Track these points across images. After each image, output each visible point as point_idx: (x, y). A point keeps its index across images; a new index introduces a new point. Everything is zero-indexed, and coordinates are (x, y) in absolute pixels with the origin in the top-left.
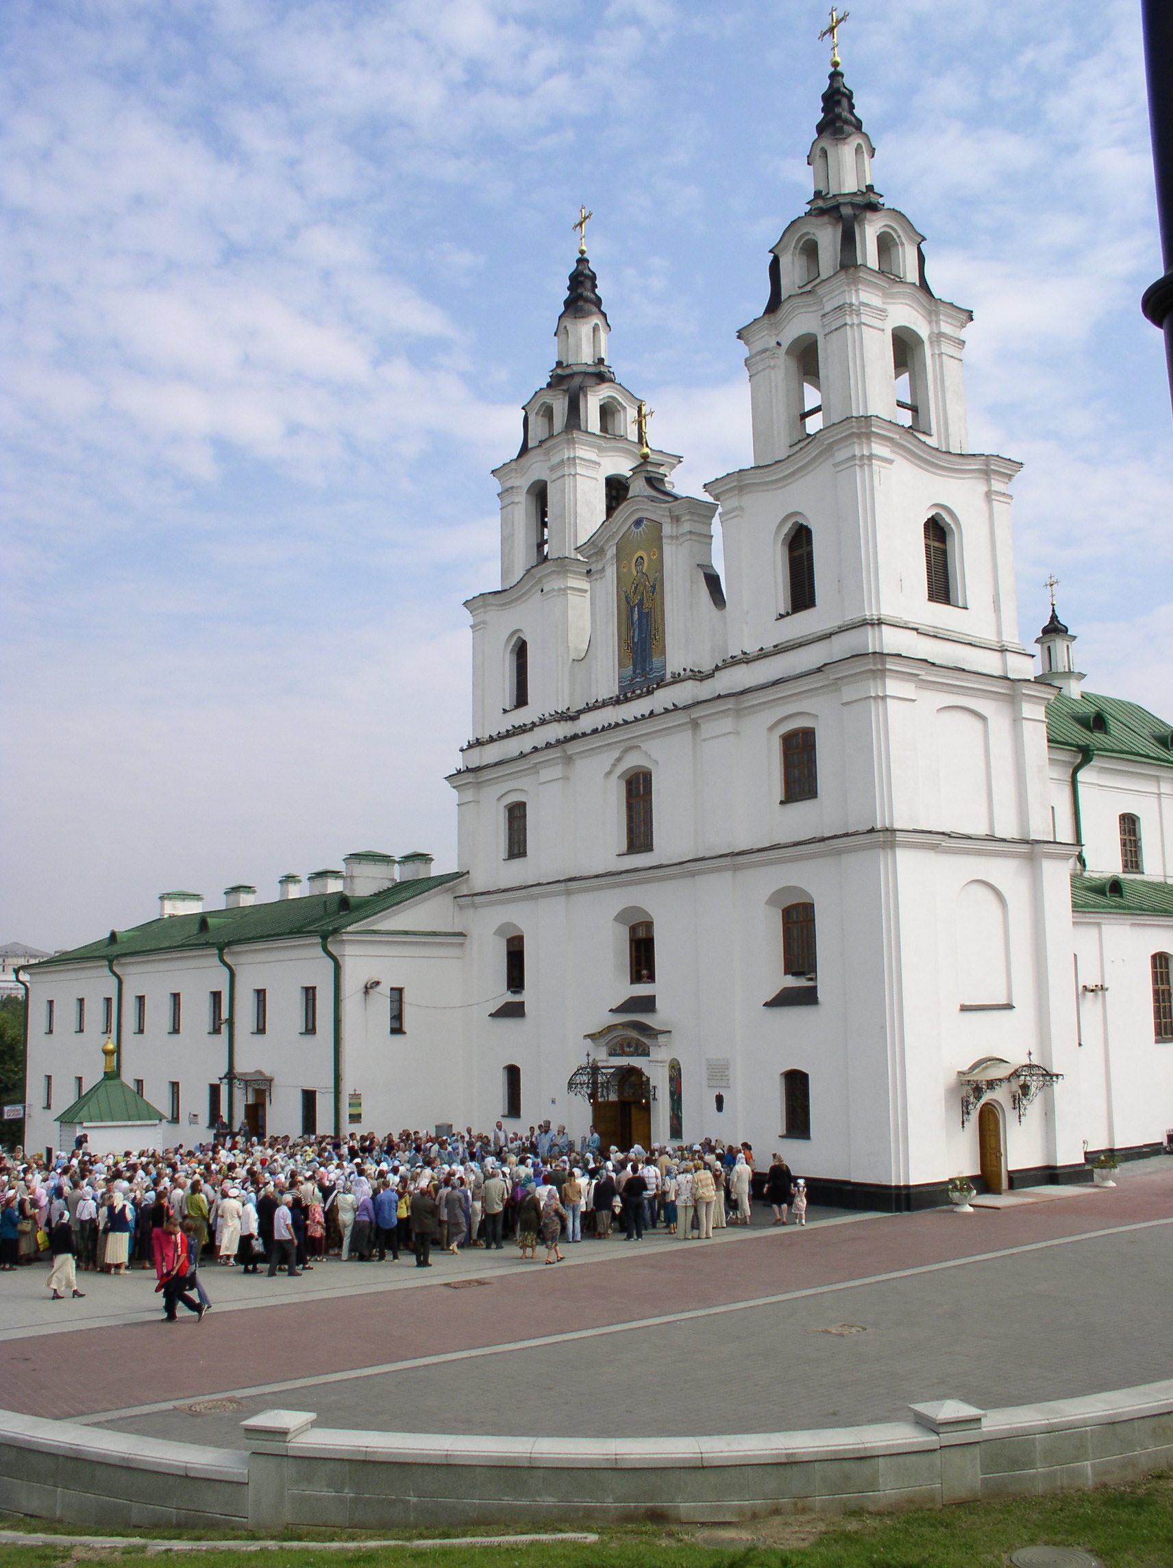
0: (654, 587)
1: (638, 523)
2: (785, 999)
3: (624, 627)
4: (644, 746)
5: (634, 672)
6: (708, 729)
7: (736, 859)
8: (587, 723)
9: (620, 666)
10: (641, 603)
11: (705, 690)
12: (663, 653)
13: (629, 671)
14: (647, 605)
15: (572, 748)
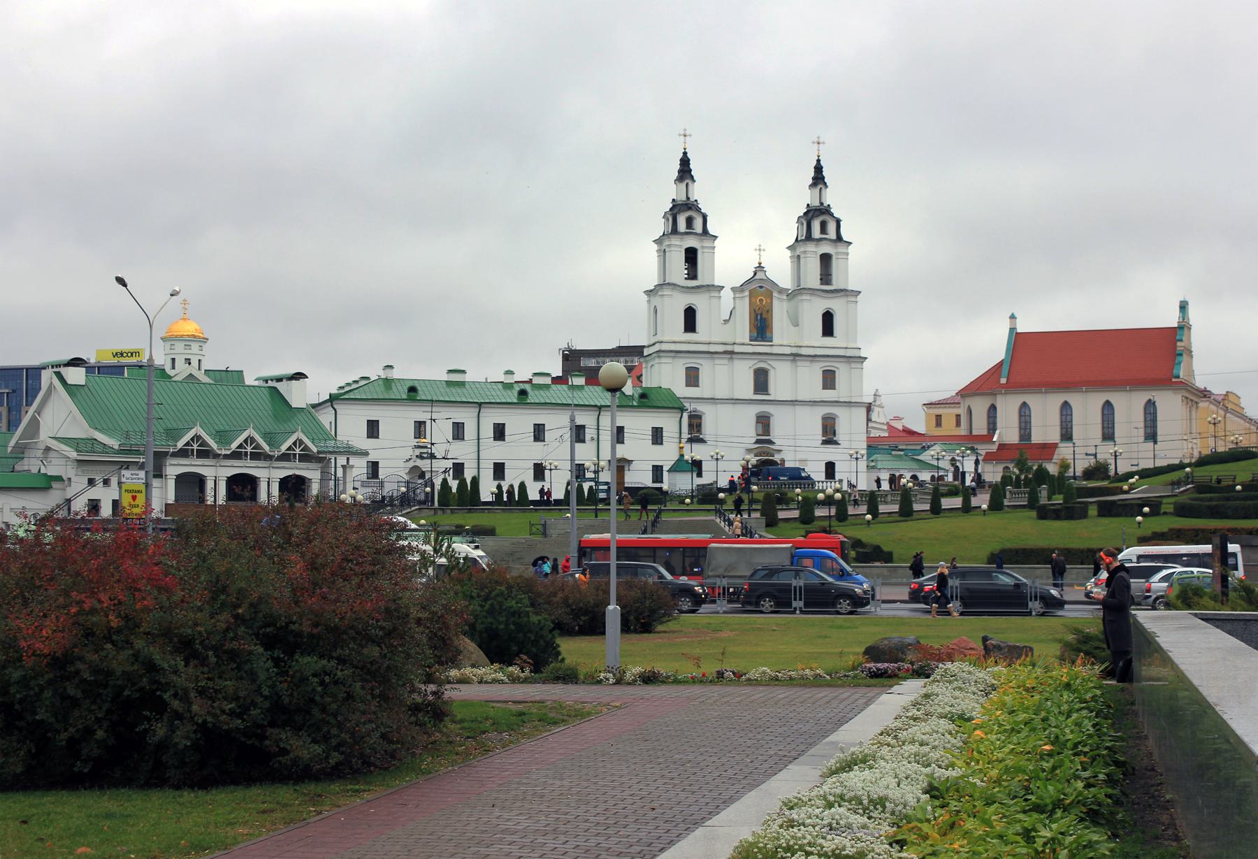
0: (768, 311)
1: (761, 287)
2: (825, 442)
3: (753, 322)
4: (769, 362)
5: (758, 337)
6: (799, 363)
7: (814, 403)
8: (737, 349)
9: (751, 331)
10: (761, 314)
11: (794, 351)
12: (772, 333)
13: (755, 334)
14: (764, 316)
15: (734, 356)
